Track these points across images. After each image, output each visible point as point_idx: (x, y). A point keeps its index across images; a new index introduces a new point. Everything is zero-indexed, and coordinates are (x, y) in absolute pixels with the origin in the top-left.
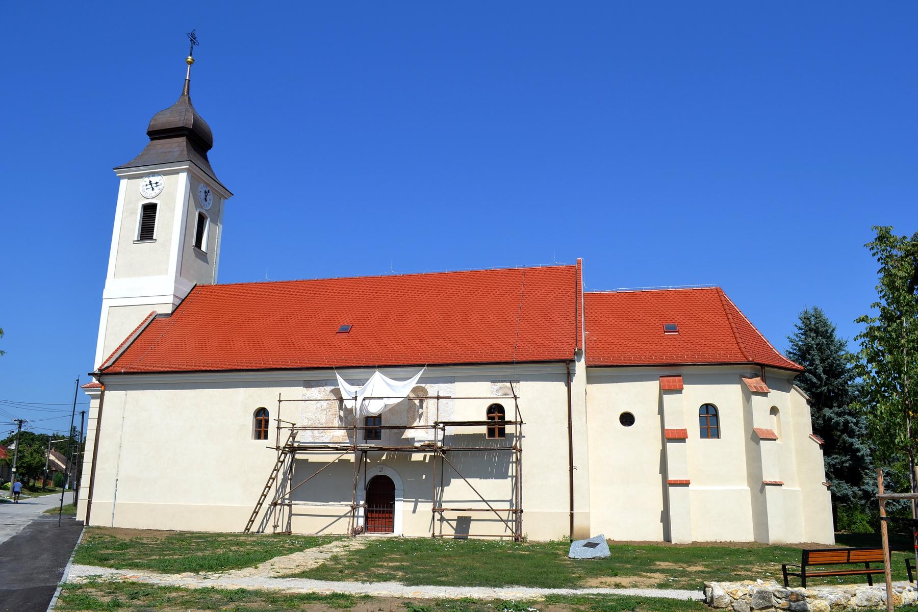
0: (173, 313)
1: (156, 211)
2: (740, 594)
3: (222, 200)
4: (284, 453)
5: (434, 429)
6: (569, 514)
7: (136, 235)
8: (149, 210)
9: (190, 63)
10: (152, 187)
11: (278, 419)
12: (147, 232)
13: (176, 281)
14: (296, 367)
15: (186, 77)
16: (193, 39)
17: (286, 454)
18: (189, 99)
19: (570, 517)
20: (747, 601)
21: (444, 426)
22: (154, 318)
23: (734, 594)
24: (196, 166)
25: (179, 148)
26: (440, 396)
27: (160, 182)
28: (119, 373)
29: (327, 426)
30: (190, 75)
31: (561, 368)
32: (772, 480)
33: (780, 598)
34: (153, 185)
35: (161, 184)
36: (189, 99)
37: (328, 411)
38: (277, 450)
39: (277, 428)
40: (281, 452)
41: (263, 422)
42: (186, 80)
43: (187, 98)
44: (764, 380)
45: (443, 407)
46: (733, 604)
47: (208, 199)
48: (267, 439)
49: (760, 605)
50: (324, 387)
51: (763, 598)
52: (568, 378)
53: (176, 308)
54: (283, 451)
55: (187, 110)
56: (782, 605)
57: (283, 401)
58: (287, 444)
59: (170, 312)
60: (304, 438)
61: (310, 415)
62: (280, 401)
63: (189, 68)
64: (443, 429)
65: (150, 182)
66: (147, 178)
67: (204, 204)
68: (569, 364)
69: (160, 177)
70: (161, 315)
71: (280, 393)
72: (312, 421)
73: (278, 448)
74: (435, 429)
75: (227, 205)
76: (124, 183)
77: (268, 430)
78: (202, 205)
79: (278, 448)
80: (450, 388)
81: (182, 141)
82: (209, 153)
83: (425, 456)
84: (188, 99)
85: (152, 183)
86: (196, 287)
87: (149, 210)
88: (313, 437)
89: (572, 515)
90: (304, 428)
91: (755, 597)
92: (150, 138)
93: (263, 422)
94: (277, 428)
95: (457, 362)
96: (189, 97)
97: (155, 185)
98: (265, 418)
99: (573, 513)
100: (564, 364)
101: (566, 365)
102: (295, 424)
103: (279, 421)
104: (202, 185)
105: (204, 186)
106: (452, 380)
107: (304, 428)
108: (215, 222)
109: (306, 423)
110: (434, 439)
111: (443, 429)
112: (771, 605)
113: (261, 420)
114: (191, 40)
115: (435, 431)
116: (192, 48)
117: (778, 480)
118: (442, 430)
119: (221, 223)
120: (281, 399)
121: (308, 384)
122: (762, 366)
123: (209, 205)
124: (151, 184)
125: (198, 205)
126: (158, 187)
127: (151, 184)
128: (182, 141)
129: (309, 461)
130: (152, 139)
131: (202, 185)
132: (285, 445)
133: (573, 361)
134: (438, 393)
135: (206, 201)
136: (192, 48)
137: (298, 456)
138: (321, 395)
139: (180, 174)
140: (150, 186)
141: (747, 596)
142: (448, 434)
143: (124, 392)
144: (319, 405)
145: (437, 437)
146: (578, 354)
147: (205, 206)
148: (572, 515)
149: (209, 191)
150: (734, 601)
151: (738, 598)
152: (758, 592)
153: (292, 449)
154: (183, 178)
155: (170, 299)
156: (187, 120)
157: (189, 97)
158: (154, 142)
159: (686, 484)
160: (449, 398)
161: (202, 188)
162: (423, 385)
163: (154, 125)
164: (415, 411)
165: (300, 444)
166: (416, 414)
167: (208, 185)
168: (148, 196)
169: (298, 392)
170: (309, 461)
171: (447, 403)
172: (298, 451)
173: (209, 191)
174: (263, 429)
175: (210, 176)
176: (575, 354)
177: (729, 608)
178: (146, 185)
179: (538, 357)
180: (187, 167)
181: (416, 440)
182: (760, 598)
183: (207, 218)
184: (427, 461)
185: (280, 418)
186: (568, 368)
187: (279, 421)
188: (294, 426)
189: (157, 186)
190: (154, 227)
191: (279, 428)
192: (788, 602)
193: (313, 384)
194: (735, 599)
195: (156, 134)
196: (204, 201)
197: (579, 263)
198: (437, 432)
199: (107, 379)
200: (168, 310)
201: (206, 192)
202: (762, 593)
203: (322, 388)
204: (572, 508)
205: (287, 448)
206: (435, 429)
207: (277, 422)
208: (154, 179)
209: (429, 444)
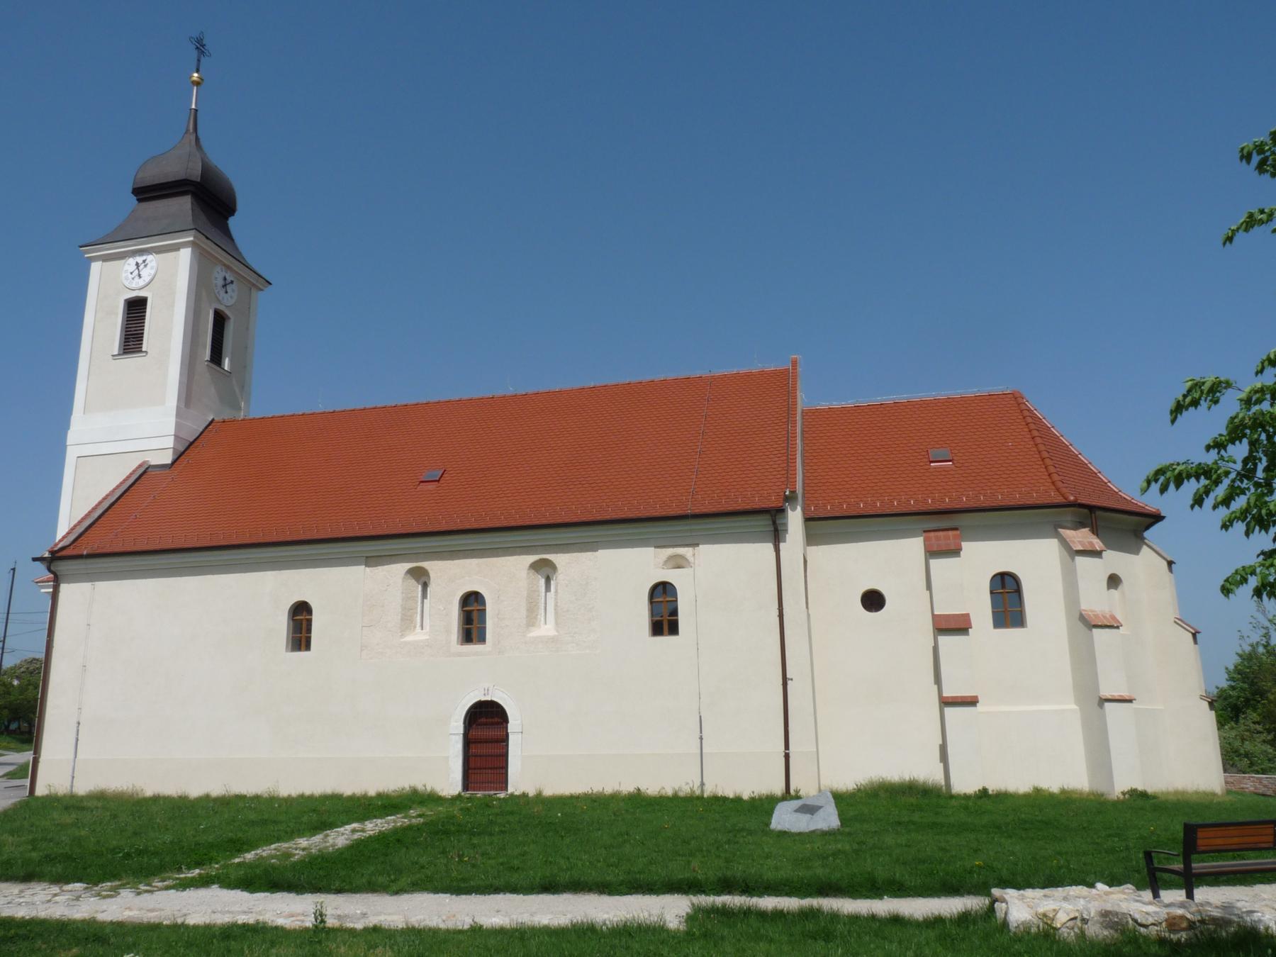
0: (174, 462)
1: (146, 308)
3: (254, 291)
6: (784, 754)
7: (115, 347)
8: (136, 308)
9: (197, 84)
12: (132, 340)
13: (179, 414)
15: (191, 105)
16: (200, 47)
24: (207, 238)
31: (763, 522)
32: (1116, 694)
41: (304, 625)
42: (191, 109)
44: (1095, 531)
48: (308, 647)
52: (777, 535)
59: (169, 461)
67: (223, 298)
76: (96, 267)
78: (220, 298)
81: (184, 205)
82: (232, 222)
86: (213, 424)
87: (136, 308)
89: (787, 757)
92: (138, 200)
93: (304, 625)
100: (768, 517)
116: (199, 60)
117: (1125, 694)
122: (1092, 508)
128: (184, 205)
130: (140, 200)
133: (781, 511)
136: (199, 60)
143: (90, 583)
148: (787, 757)
154: (185, 255)
155: (169, 442)
156: (195, 173)
159: (971, 702)
161: (218, 274)
167: (228, 268)
168: (134, 286)
174: (304, 635)
176: (787, 499)
180: (191, 239)
186: (774, 523)
190: (143, 334)
195: (145, 193)
196: (222, 292)
197: (794, 363)
199: (62, 567)
200: (167, 459)
204: (787, 746)
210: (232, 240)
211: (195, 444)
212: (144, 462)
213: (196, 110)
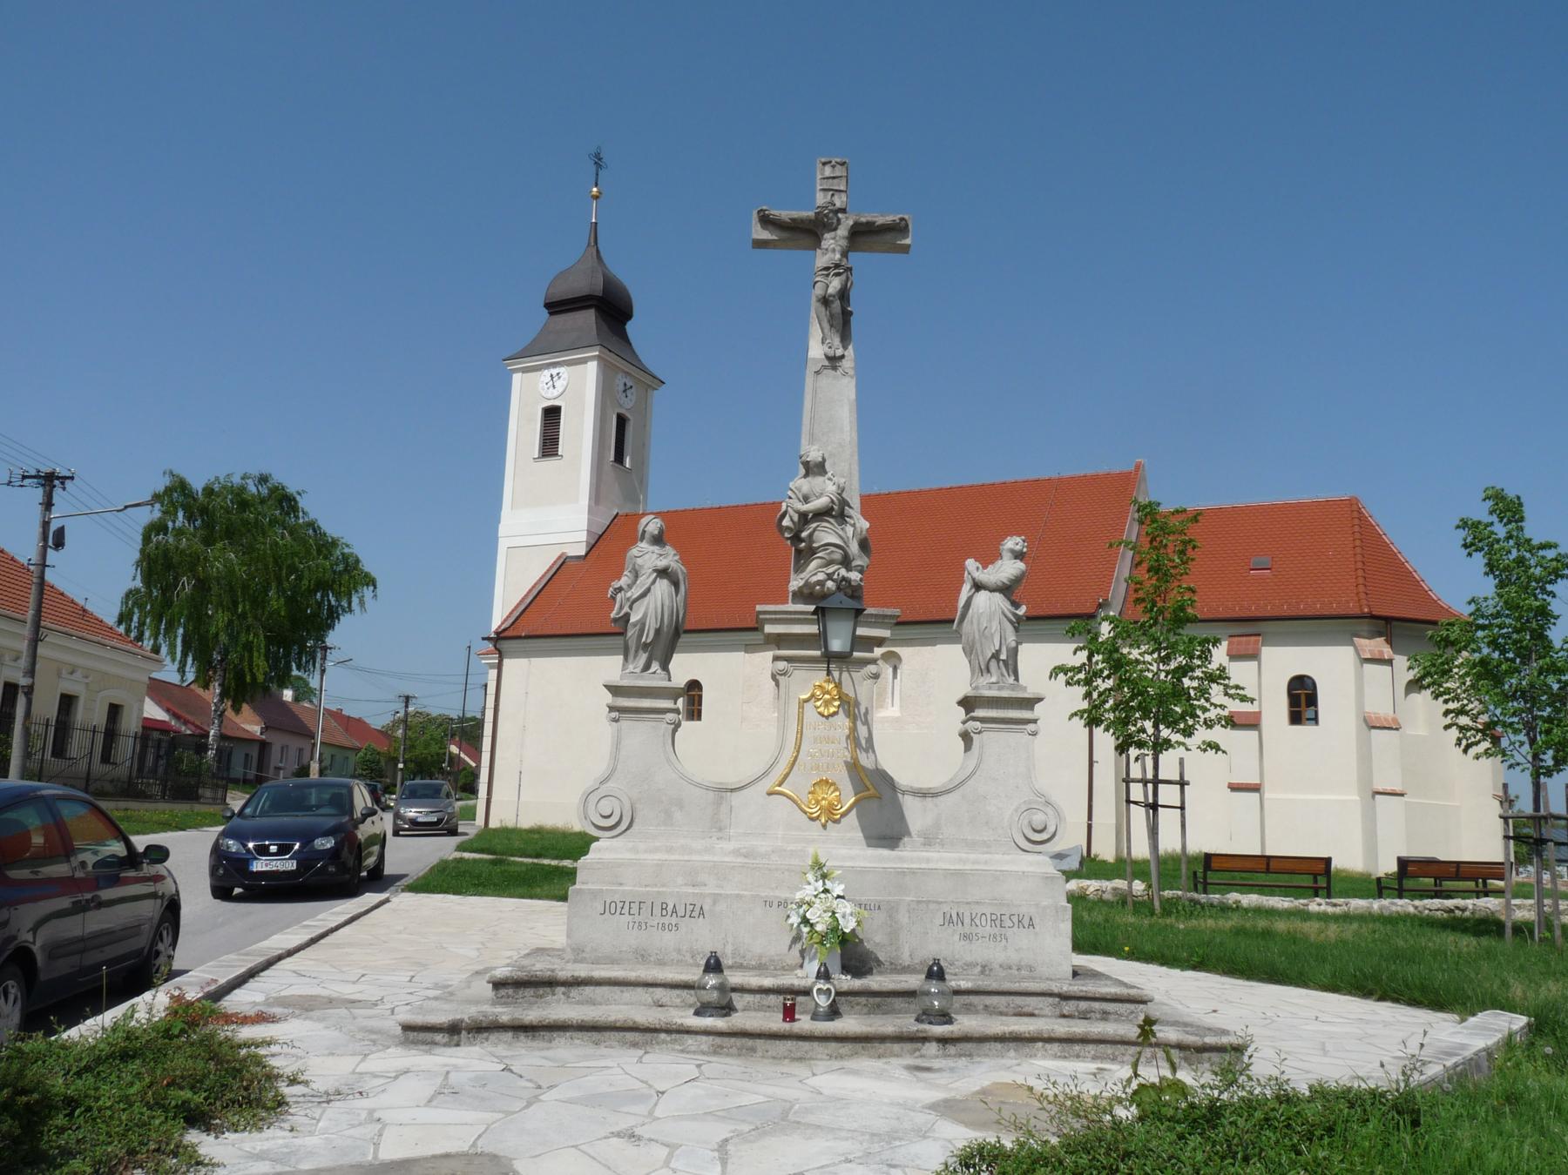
3: (650, 391)
8: (552, 415)
9: (596, 197)
12: (549, 445)
13: (590, 511)
16: (598, 161)
22: (564, 562)
28: (519, 637)
32: (1389, 788)
41: (696, 698)
44: (1389, 642)
48: (699, 718)
53: (591, 548)
59: (583, 553)
70: (572, 557)
76: (517, 377)
81: (588, 318)
82: (631, 328)
87: (552, 415)
89: (1090, 827)
93: (696, 698)
104: (619, 376)
116: (597, 175)
117: (1398, 789)
121: (750, 648)
122: (1388, 620)
128: (588, 318)
130: (551, 314)
131: (619, 376)
136: (597, 175)
143: (526, 660)
148: (1090, 827)
154: (592, 367)
155: (583, 536)
156: (598, 289)
159: (1235, 788)
161: (620, 380)
168: (549, 396)
174: (696, 707)
195: (556, 307)
199: (505, 645)
200: (581, 550)
211: (604, 537)
212: (563, 554)
213: (596, 223)
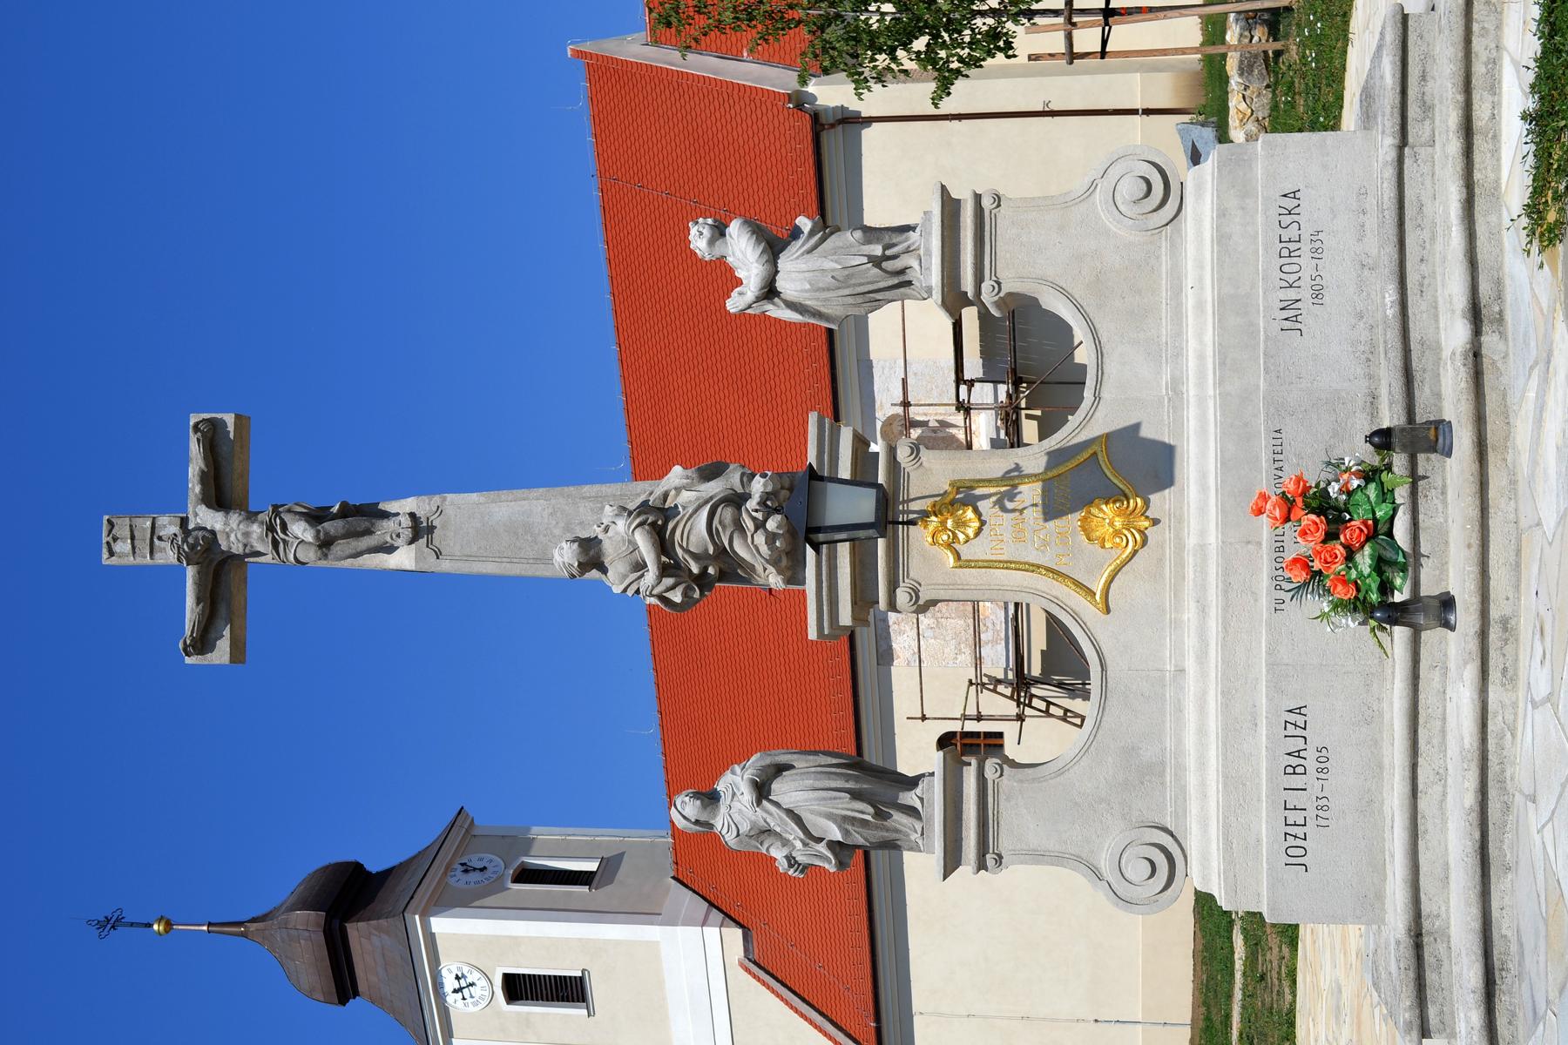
0: (741, 926)
1: (519, 975)
2: (1243, 106)
4: (1030, 701)
5: (972, 411)
6: (1145, 116)
7: (575, 1012)
8: (518, 988)
9: (169, 925)
10: (468, 986)
11: (960, 719)
13: (672, 922)
14: (849, 684)
15: (204, 931)
16: (111, 923)
17: (1033, 696)
18: (254, 920)
19: (1151, 116)
20: (1255, 95)
21: (965, 382)
22: (755, 963)
23: (1244, 117)
24: (412, 898)
25: (372, 937)
26: (902, 399)
27: (455, 972)
28: (878, 1031)
29: (971, 616)
30: (199, 922)
31: (832, 140)
33: (1252, 37)
34: (463, 983)
35: (459, 969)
36: (254, 920)
37: (939, 615)
38: (1024, 720)
39: (978, 721)
40: (1028, 711)
42: (209, 932)
43: (253, 927)
45: (924, 383)
46: (1260, 119)
47: (479, 865)
49: (1262, 74)
50: (891, 623)
51: (1251, 67)
52: (853, 122)
53: (731, 918)
54: (1025, 705)
55: (285, 926)
56: (1263, 34)
57: (923, 712)
58: (1011, 698)
59: (739, 932)
60: (997, 661)
61: (950, 650)
62: (924, 718)
63: (180, 927)
64: (971, 383)
65: (455, 991)
66: (448, 999)
67: (495, 872)
68: (823, 125)
69: (444, 972)
70: (746, 950)
71: (908, 718)
72: (962, 646)
73: (1020, 718)
74: (971, 409)
75: (485, 819)
77: (984, 732)
78: (495, 876)
79: (1020, 718)
80: (883, 368)
82: (373, 866)
83: (1028, 417)
84: (255, 924)
85: (457, 986)
86: (681, 877)
87: (518, 988)
88: (995, 642)
89: (1147, 112)
90: (978, 661)
91: (1250, 82)
92: (354, 998)
94: (978, 721)
95: (826, 360)
96: (249, 921)
97: (462, 981)
98: (958, 737)
99: (1143, 110)
100: (824, 136)
101: (825, 132)
102: (970, 681)
103: (965, 718)
104: (452, 881)
105: (452, 877)
106: (866, 367)
107: (978, 661)
108: (527, 845)
109: (967, 658)
110: (994, 412)
111: (971, 383)
112: (1262, 54)
113: (964, 745)
114: (113, 927)
115: (976, 409)
116: (132, 924)
118: (973, 385)
119: (528, 830)
120: (920, 716)
121: (885, 656)
123: (494, 861)
124: (460, 990)
125: (497, 887)
126: (466, 974)
127: (460, 990)
129: (1045, 648)
130: (356, 994)
131: (452, 881)
132: (1014, 700)
133: (816, 117)
134: (895, 405)
135: (485, 868)
136: (132, 924)
137: (1036, 671)
138: (907, 628)
139: (433, 931)
140: (464, 990)
141: (1247, 93)
142: (981, 371)
143: (916, 1020)
144: (928, 633)
145: (987, 404)
146: (800, 101)
147: (496, 869)
148: (1147, 112)
149: (462, 864)
150: (1254, 115)
151: (1250, 110)
152: (1241, 75)
153: (1021, 683)
154: (439, 924)
155: (712, 933)
156: (307, 921)
157: (249, 921)
158: (362, 987)
160: (904, 381)
161: (459, 880)
162: (879, 425)
163: (324, 994)
164: (935, 439)
165: (1011, 666)
166: (940, 434)
167: (448, 868)
168: (487, 993)
169: (902, 677)
170: (1045, 648)
171: (915, 374)
172: (1026, 672)
173: (462, 864)
174: (981, 741)
175: (430, 866)
176: (799, 106)
177: (1266, 124)
178: (464, 999)
179: (807, 165)
180: (417, 917)
181: (995, 437)
182: (1251, 72)
183: (523, 862)
184: (1038, 413)
185: (959, 717)
186: (832, 126)
187: (965, 718)
188: (974, 681)
189: (464, 976)
190: (555, 977)
191: (979, 718)
192: (1258, 26)
193: (885, 647)
194: (1252, 114)
195: (344, 985)
196: (488, 873)
197: (580, 54)
198: (976, 404)
201: (466, 871)
202: (1243, 69)
203: (893, 628)
204: (1133, 112)
205: (1019, 696)
206: (971, 409)
207: (966, 721)
208: (449, 983)
209: (1001, 420)
210: (393, 868)
211: (712, 899)
212: (742, 965)
213: (210, 924)
